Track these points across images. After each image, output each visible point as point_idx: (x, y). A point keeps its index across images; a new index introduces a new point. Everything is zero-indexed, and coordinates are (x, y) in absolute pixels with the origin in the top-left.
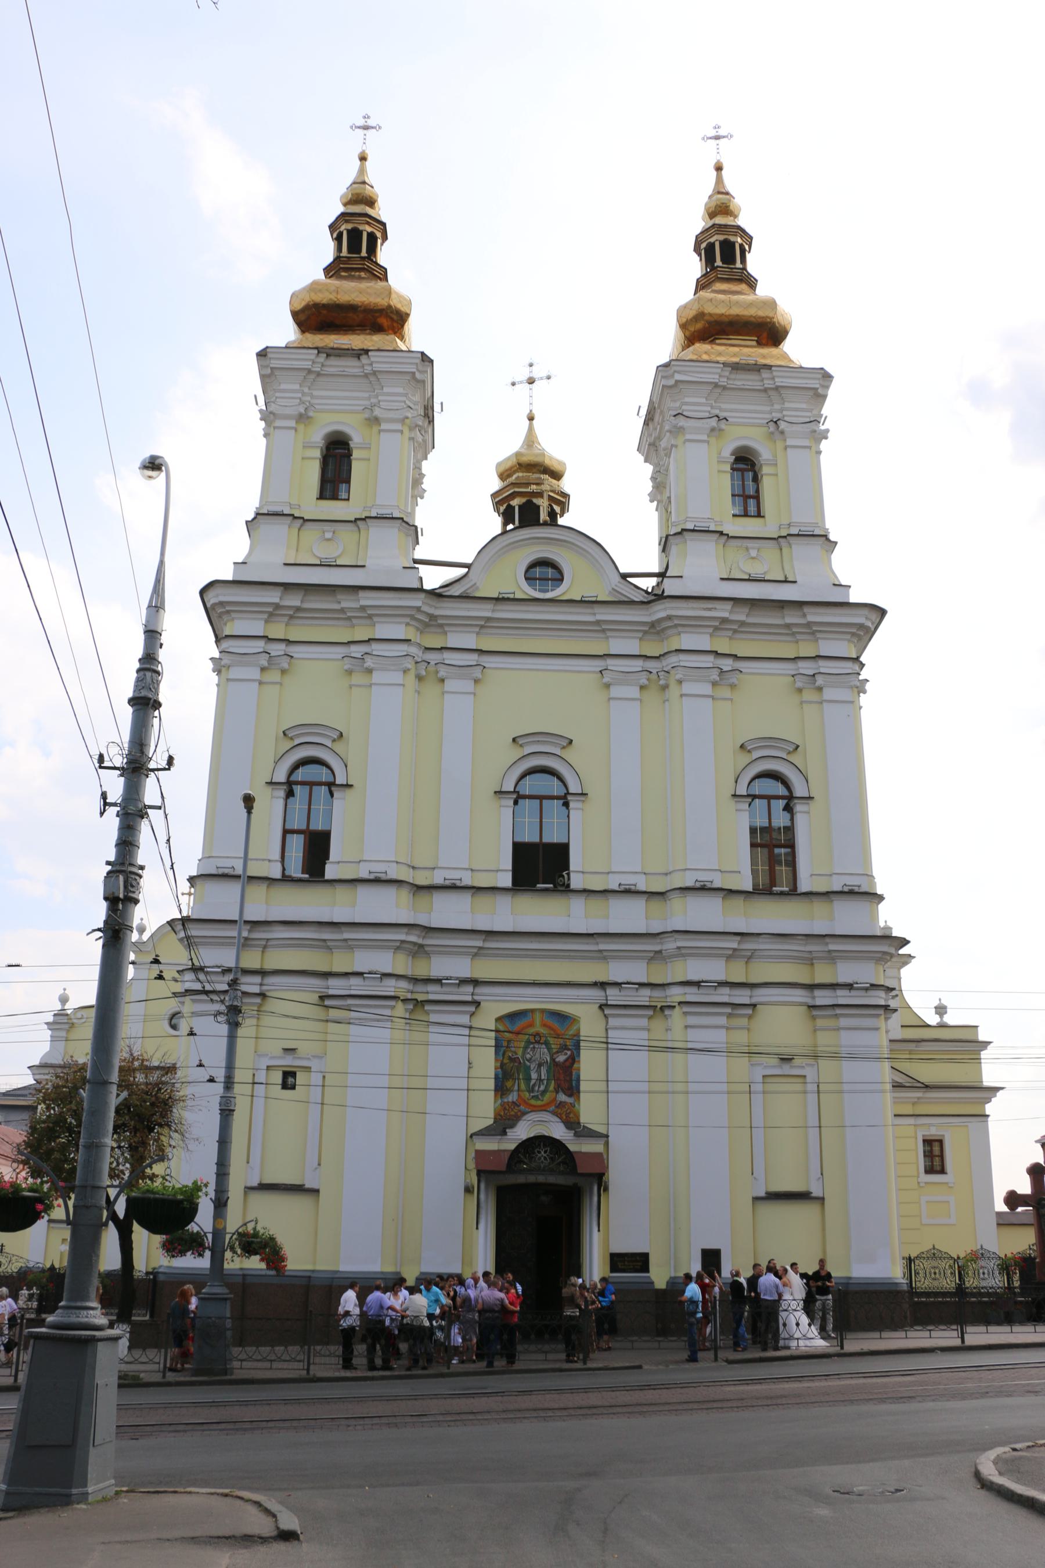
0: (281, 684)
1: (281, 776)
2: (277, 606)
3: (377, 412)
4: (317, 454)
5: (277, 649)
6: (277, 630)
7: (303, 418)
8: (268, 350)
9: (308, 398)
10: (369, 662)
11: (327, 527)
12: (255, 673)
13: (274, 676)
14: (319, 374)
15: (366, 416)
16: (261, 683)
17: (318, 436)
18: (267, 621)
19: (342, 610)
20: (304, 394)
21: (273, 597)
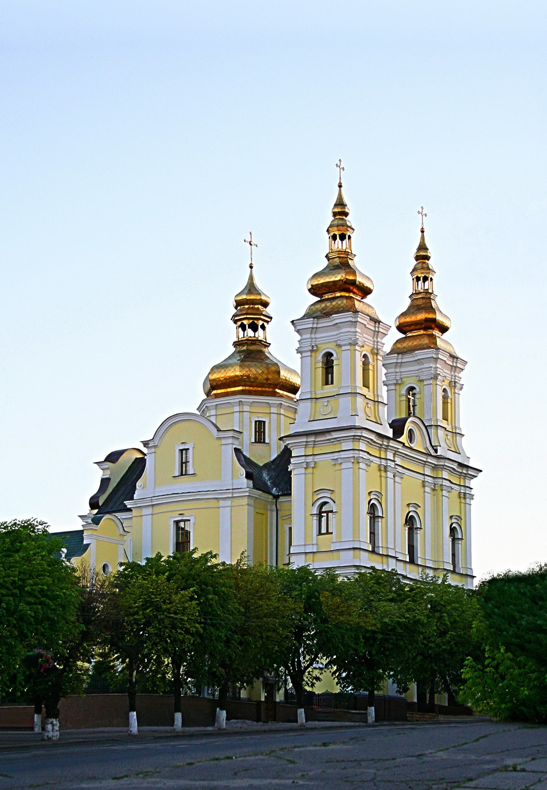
0: (313, 473)
1: (315, 511)
2: (307, 442)
3: (339, 342)
4: (320, 365)
5: (310, 459)
6: (309, 452)
7: (313, 350)
8: (295, 322)
9: (314, 340)
10: (340, 462)
11: (326, 400)
12: (303, 471)
13: (310, 470)
14: (316, 328)
15: (336, 344)
16: (305, 474)
17: (320, 357)
18: (305, 448)
19: (328, 440)
20: (312, 338)
21: (304, 439)
